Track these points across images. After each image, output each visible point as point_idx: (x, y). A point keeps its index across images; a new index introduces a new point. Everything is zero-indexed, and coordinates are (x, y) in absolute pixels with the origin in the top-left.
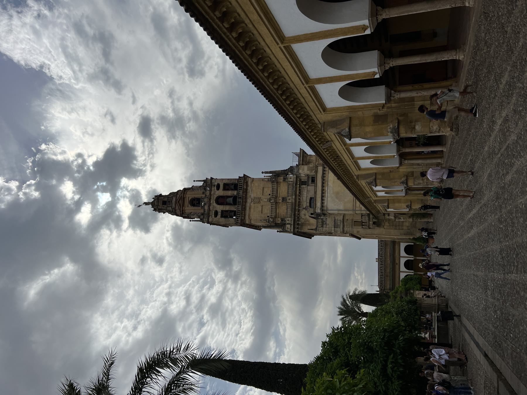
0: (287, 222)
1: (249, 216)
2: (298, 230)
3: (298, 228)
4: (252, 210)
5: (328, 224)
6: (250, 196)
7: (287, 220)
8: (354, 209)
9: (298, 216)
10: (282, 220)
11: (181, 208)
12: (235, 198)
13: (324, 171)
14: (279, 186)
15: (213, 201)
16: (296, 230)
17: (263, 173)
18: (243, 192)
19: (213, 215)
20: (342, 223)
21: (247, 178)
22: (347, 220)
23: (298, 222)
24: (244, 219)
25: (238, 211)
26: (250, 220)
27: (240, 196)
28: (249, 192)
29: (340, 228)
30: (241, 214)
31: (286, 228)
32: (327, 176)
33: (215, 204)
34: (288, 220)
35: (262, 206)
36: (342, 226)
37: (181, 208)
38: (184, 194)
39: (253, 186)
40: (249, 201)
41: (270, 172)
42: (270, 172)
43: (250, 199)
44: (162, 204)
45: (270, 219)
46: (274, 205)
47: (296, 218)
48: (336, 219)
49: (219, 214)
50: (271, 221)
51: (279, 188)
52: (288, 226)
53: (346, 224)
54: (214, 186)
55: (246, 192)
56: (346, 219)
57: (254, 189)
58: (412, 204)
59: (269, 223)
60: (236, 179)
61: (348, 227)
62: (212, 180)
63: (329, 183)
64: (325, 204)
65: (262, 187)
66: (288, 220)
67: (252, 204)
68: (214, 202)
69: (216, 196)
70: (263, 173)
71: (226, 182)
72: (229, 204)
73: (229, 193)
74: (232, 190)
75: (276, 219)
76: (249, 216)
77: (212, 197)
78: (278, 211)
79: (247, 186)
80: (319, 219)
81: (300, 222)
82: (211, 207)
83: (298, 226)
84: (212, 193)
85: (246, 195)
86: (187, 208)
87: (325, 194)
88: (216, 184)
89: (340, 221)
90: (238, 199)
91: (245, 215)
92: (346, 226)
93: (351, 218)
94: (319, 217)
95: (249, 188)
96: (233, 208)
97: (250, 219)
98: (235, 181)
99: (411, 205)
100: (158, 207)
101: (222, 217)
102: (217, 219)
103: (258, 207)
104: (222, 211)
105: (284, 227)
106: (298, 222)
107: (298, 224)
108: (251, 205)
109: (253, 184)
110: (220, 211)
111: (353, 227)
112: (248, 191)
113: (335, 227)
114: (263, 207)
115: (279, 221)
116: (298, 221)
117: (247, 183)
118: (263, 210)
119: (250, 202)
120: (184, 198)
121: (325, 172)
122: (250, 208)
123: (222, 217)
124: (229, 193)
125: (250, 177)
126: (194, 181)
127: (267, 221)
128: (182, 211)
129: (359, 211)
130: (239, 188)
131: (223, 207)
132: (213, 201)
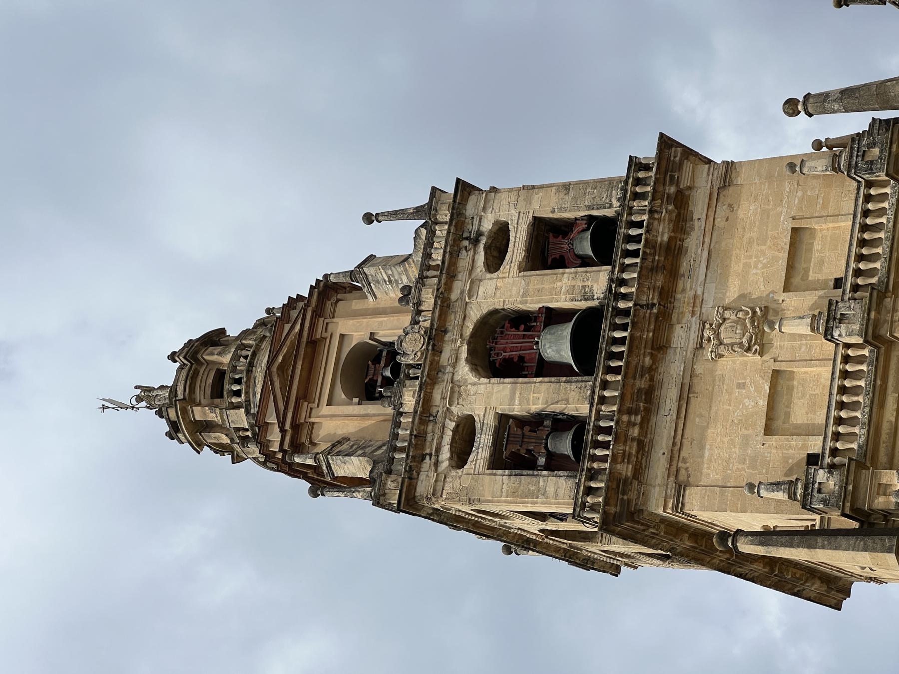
6: (697, 301)
17: (791, 107)
18: (646, 272)
19: (445, 454)
21: (688, 166)
25: (599, 417)
27: (622, 305)
30: (616, 439)
33: (464, 371)
37: (286, 408)
38: (319, 313)
42: (845, 92)
44: (208, 392)
45: (821, 475)
46: (860, 360)
49: (484, 441)
54: (476, 242)
55: (673, 274)
60: (610, 183)
65: (790, 225)
68: (464, 354)
69: (475, 314)
74: (585, 262)
75: (866, 474)
76: (675, 450)
77: (454, 320)
82: (437, 396)
84: (454, 296)
85: (667, 295)
88: (487, 226)
90: (615, 327)
91: (644, 447)
95: (693, 242)
97: (682, 476)
100: (184, 411)
101: (496, 462)
102: (466, 482)
104: (503, 419)
109: (722, 211)
110: (491, 421)
112: (684, 266)
117: (681, 200)
123: (496, 462)
125: (709, 161)
126: (369, 218)
127: (792, 496)
128: (296, 427)
130: (621, 245)
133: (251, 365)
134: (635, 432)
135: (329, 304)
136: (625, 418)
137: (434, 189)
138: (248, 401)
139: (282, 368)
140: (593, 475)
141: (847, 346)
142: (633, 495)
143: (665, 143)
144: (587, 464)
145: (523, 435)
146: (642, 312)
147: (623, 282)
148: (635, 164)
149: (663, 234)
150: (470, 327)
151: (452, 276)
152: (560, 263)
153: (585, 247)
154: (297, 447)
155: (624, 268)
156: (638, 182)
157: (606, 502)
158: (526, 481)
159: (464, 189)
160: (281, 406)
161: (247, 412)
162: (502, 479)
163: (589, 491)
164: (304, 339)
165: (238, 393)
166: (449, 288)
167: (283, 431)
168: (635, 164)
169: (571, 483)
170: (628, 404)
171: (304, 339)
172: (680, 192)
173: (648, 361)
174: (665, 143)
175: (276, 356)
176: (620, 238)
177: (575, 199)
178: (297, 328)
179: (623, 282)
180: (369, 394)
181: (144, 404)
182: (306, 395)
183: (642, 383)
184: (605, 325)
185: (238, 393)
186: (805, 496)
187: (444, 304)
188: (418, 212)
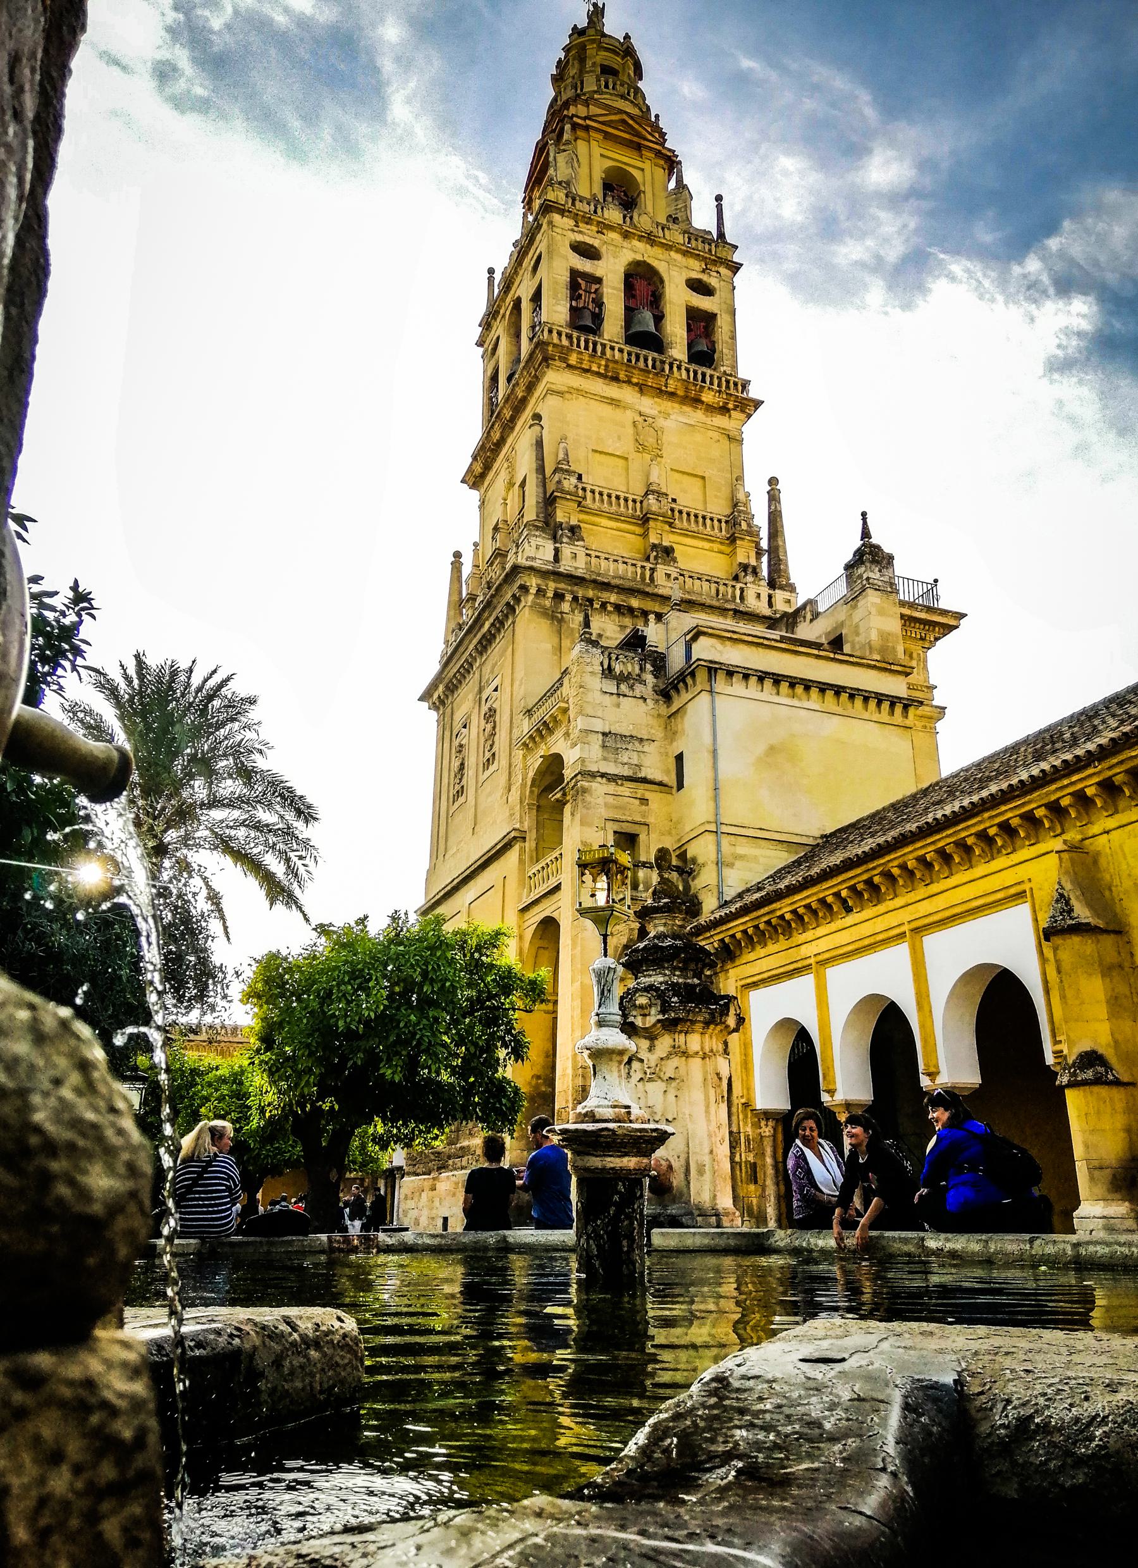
0: (566, 551)
1: (579, 391)
2: (533, 591)
3: (540, 592)
4: (607, 410)
5: (618, 705)
7: (575, 549)
8: (725, 829)
9: (596, 606)
10: (574, 531)
11: (603, 123)
12: (654, 342)
13: (892, 705)
14: (716, 546)
15: (639, 251)
16: (533, 582)
17: (773, 481)
19: (580, 238)
20: (626, 772)
21: (743, 416)
22: (644, 801)
23: (569, 597)
24: (569, 366)
26: (560, 393)
28: (683, 413)
29: (605, 759)
31: (540, 541)
32: (866, 715)
34: (575, 556)
35: (626, 459)
36: (611, 769)
38: (658, 154)
39: (710, 433)
40: (648, 404)
41: (775, 518)
43: (654, 412)
47: (590, 594)
48: (646, 749)
50: (566, 483)
51: (707, 545)
52: (546, 551)
53: (626, 789)
56: (648, 795)
57: (698, 437)
58: (1117, 1094)
59: (554, 472)
60: (734, 367)
61: (610, 799)
62: (728, 267)
63: (836, 719)
64: (738, 687)
65: (706, 475)
66: (575, 556)
67: (630, 416)
68: (639, 258)
69: (661, 267)
70: (773, 481)
71: (722, 321)
72: (630, 313)
73: (676, 330)
77: (657, 251)
78: (605, 522)
79: (710, 409)
80: (642, 669)
81: (566, 607)
83: (550, 594)
84: (672, 253)
86: (597, 150)
87: (788, 696)
89: (639, 766)
92: (612, 788)
93: (651, 820)
94: (649, 667)
96: (613, 327)
97: (567, 396)
98: (726, 362)
99: (1117, 1083)
101: (575, 274)
103: (619, 438)
105: (542, 529)
106: (569, 597)
107: (559, 597)
108: (628, 412)
109: (716, 435)
110: (598, 274)
111: (609, 825)
113: (604, 734)
114: (621, 462)
115: (564, 514)
116: (575, 599)
117: (724, 410)
118: (603, 458)
119: (643, 410)
120: (638, 148)
121: (886, 705)
122: (614, 402)
123: (575, 274)
124: (676, 330)
128: (587, 128)
129: (719, 851)
130: (701, 370)
131: (614, 288)
132: (639, 251)
133: (622, 97)
134: (595, 368)
135: (662, 162)
136: (603, 363)
137: (736, 247)
138: (602, 93)
139: (624, 121)
140: (569, 337)
141: (641, 502)
142: (557, 363)
143: (758, 404)
144: (575, 334)
145: (590, 293)
146: (663, 380)
147: (679, 368)
148: (745, 385)
149: (708, 397)
150: (655, 263)
151: (685, 253)
152: (689, 329)
153: (703, 346)
154: (575, 126)
155: (688, 370)
156: (736, 384)
157: (555, 345)
158: (564, 293)
159: (736, 268)
160: (601, 119)
161: (595, 92)
162: (565, 277)
163: (559, 334)
164: (643, 142)
165: (606, 86)
166: (678, 251)
167: (585, 118)
168: (745, 385)
169: (563, 323)
170: (611, 365)
171: (643, 142)
172: (728, 410)
173: (635, 380)
174: (758, 404)
175: (632, 118)
176: (704, 369)
177: (727, 342)
178: (650, 137)
179: (679, 368)
180: (607, 187)
181: (592, 9)
182: (607, 136)
183: (622, 376)
184: (656, 355)
185: (606, 86)
186: (562, 469)
187: (668, 247)
188: (721, 235)
